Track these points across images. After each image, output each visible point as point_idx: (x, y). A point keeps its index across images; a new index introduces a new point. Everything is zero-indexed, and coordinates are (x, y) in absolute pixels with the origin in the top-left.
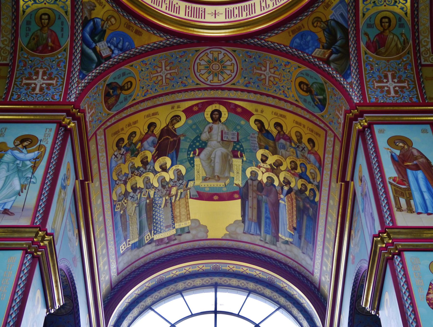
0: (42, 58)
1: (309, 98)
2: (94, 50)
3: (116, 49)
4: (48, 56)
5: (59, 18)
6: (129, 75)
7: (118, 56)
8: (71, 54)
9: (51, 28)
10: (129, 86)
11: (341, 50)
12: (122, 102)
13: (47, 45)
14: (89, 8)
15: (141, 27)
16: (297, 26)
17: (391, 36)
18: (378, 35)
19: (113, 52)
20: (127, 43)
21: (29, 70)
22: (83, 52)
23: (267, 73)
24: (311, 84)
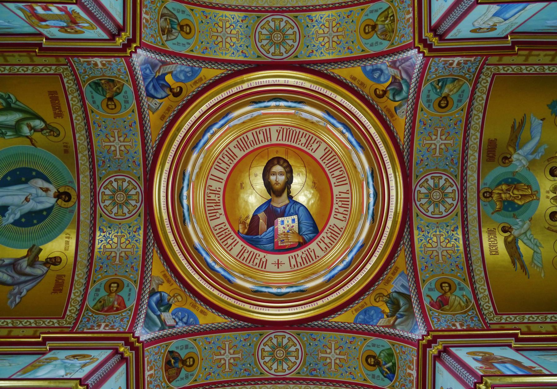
0: (107, 315)
1: (377, 372)
2: (159, 317)
3: (180, 321)
4: (112, 314)
5: (128, 286)
6: (192, 350)
7: (181, 328)
8: (136, 314)
9: (118, 294)
10: (191, 363)
11: (405, 313)
12: (182, 379)
13: (112, 307)
14: (157, 282)
15: (207, 309)
16: (360, 305)
17: (454, 297)
18: (440, 296)
19: (177, 323)
20: (192, 320)
21: (92, 324)
22: (147, 315)
23: (333, 356)
24: (378, 355)
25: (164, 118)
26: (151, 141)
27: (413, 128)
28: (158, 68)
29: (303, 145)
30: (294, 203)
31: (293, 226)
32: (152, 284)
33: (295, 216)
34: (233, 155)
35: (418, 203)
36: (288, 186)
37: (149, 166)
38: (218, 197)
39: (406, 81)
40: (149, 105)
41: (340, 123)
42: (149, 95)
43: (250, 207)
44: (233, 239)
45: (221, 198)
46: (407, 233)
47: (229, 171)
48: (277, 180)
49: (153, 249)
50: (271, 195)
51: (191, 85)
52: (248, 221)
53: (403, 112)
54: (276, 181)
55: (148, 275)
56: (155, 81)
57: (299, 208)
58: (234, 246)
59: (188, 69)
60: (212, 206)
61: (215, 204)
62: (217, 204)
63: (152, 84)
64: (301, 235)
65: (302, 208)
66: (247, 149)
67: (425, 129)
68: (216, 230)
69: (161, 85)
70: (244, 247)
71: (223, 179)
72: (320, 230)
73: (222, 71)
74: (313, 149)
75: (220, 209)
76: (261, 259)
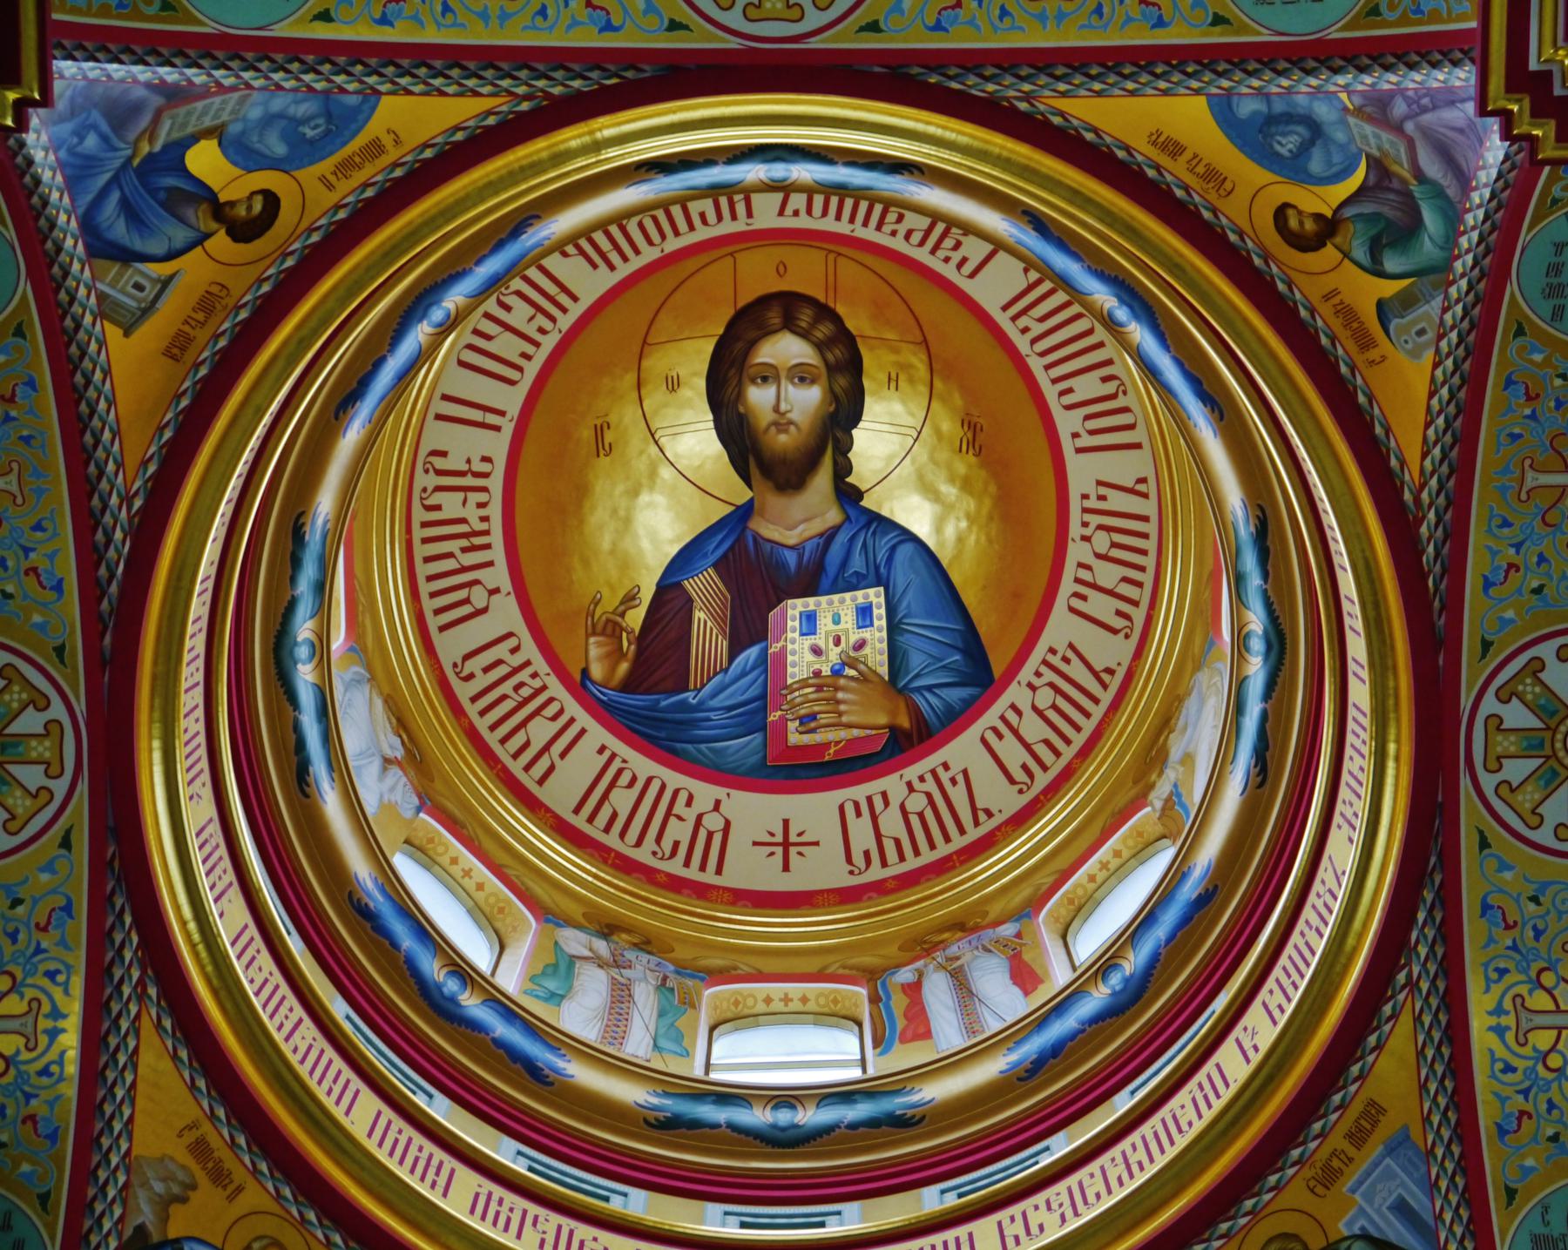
14: (159, 1187)
25: (183, 349)
26: (120, 465)
27: (1470, 411)
28: (145, 121)
29: (916, 238)
30: (868, 525)
31: (860, 645)
32: (131, 1202)
33: (871, 591)
34: (552, 289)
35: (1488, 782)
36: (839, 434)
37: (114, 588)
38: (481, 505)
39: (1439, 193)
40: (102, 297)
41: (1101, 276)
42: (102, 249)
43: (645, 544)
44: (554, 718)
45: (495, 511)
46: (1430, 933)
47: (532, 369)
48: (783, 407)
49: (138, 1016)
50: (748, 481)
51: (323, 179)
52: (636, 618)
53: (1421, 332)
54: (776, 409)
55: (114, 1160)
56: (131, 180)
57: (893, 549)
58: (563, 755)
59: (303, 109)
60: (450, 555)
61: (464, 543)
62: (474, 540)
63: (115, 196)
64: (900, 691)
65: (906, 550)
66: (625, 259)
67: (1533, 416)
68: (471, 676)
69: (162, 195)
70: (613, 756)
71: (502, 413)
72: (998, 670)
73: (488, 103)
74: (964, 261)
75: (490, 564)
76: (700, 817)
